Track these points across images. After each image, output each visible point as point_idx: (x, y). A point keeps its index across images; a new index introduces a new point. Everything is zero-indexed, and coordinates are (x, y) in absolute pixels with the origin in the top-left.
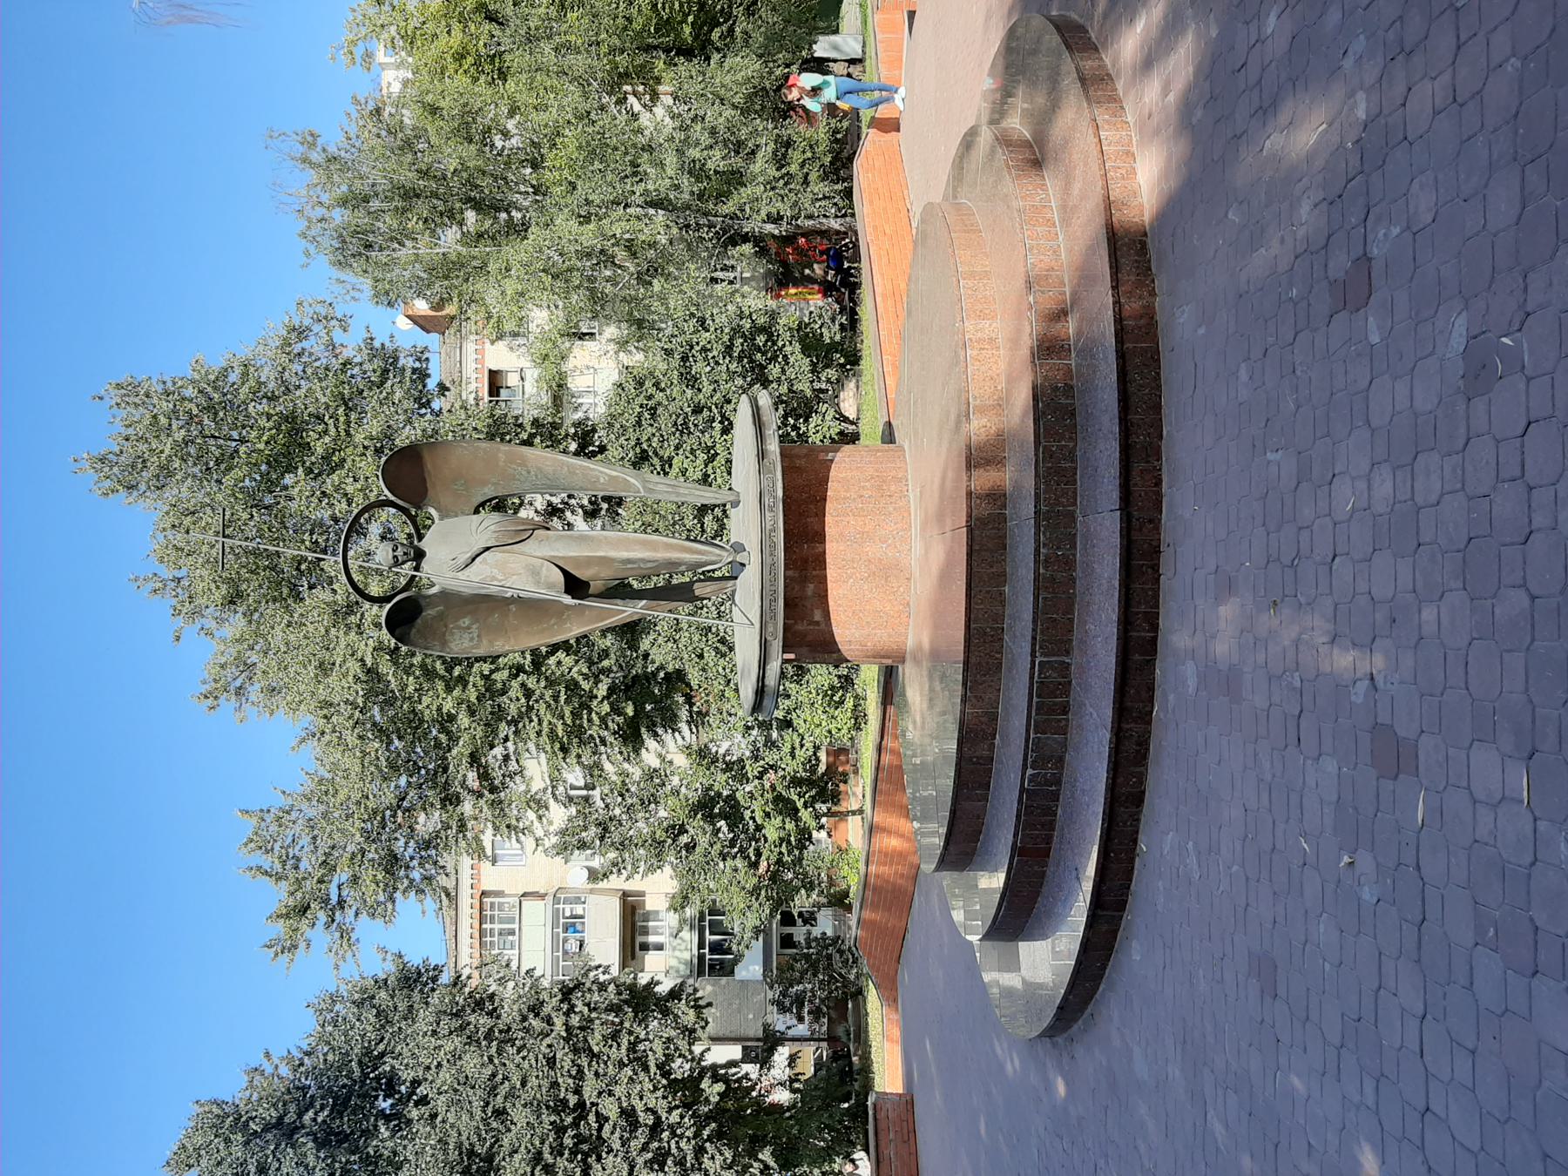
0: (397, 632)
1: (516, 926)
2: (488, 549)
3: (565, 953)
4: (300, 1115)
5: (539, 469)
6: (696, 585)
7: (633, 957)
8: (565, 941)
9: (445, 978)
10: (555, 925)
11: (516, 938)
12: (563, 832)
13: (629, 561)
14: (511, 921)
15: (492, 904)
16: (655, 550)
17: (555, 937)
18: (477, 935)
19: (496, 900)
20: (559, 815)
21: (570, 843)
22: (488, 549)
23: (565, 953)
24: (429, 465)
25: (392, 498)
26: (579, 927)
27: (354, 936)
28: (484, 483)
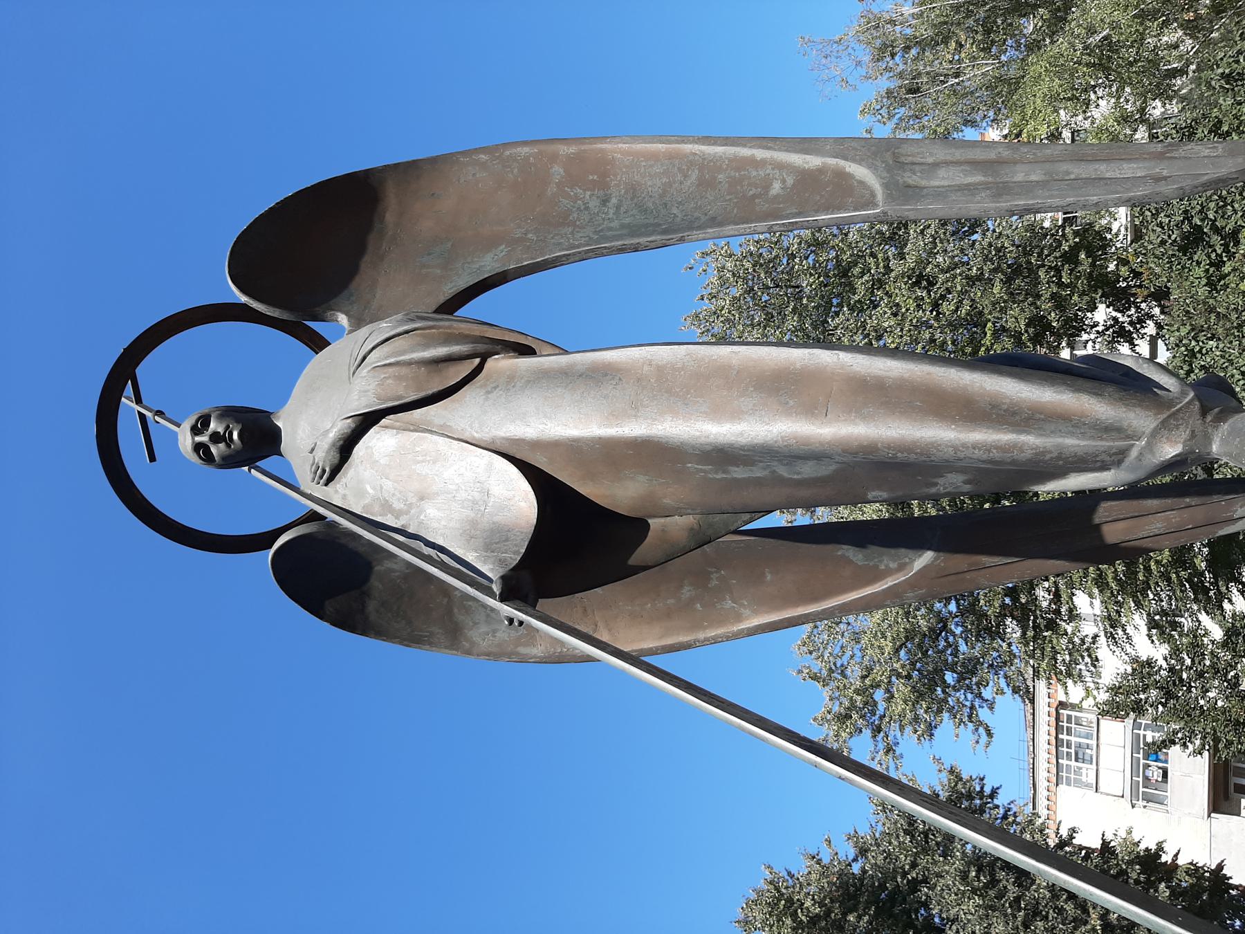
0: (329, 606)
1: (1093, 742)
2: (367, 421)
3: (1146, 778)
4: (845, 914)
5: (633, 189)
6: (1104, 511)
7: (1227, 797)
8: (1147, 766)
9: (1001, 800)
10: (1135, 748)
11: (1094, 753)
12: (1114, 690)
13: (723, 455)
14: (1088, 736)
15: (1069, 717)
16: (811, 410)
17: (1135, 763)
18: (1054, 742)
19: (1073, 713)
20: (1112, 666)
21: (1122, 703)
22: (367, 421)
23: (1146, 778)
24: (390, 218)
25: (244, 299)
26: (1162, 757)
27: (898, 751)
28: (490, 243)
